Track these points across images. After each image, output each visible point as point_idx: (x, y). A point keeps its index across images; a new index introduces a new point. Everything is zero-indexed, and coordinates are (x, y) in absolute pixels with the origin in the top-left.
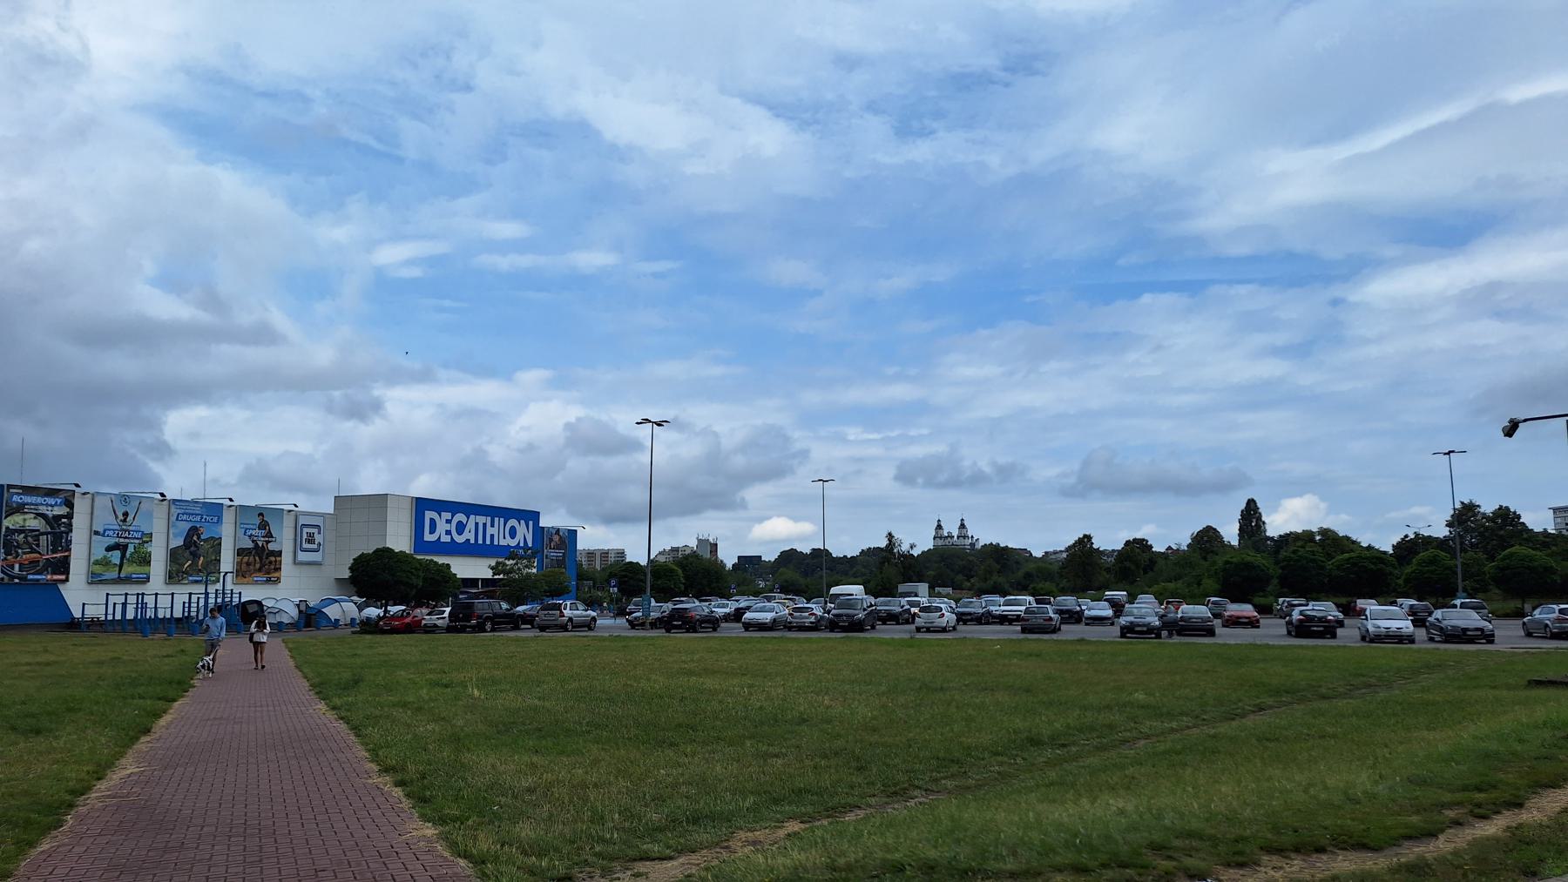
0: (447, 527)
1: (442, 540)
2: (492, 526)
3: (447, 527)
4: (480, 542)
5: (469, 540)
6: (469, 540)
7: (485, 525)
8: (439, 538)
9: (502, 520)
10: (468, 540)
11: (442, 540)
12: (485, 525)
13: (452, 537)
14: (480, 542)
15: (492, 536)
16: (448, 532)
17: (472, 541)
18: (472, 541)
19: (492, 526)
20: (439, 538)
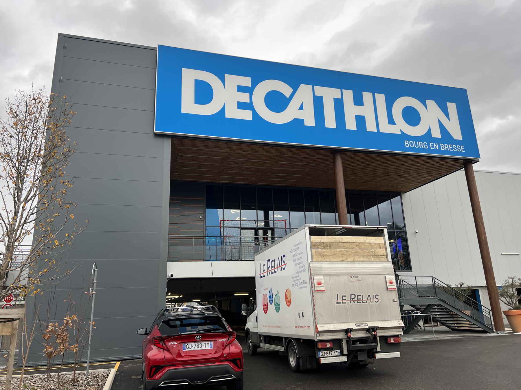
0: (245, 98)
1: (229, 115)
2: (358, 101)
3: (245, 98)
4: (330, 122)
5: (302, 121)
6: (302, 121)
7: (339, 104)
8: (223, 109)
9: (381, 98)
10: (298, 123)
11: (229, 115)
12: (339, 104)
13: (255, 114)
14: (330, 122)
15: (360, 120)
16: (241, 106)
17: (310, 121)
18: (310, 121)
19: (358, 101)
20: (223, 109)
